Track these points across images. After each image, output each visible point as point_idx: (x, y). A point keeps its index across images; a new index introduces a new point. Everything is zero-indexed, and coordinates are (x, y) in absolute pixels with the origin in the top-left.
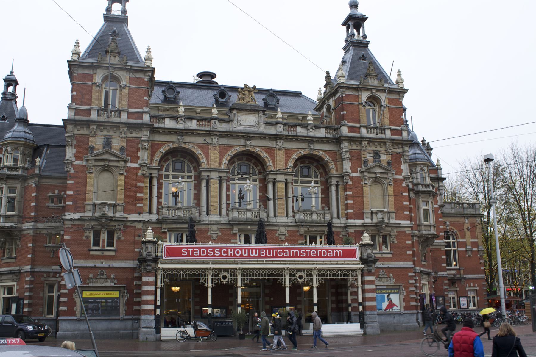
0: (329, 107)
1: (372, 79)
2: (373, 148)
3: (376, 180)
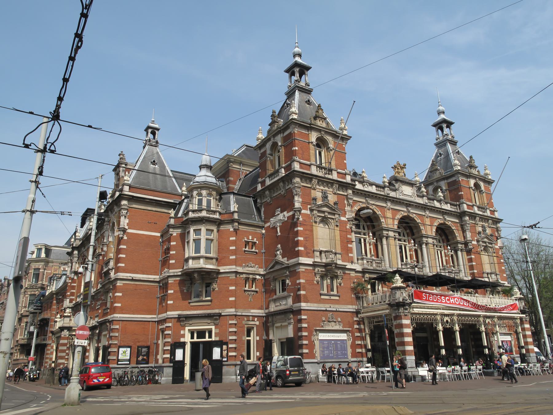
0: (275, 145)
1: (321, 121)
2: (322, 188)
3: (324, 220)
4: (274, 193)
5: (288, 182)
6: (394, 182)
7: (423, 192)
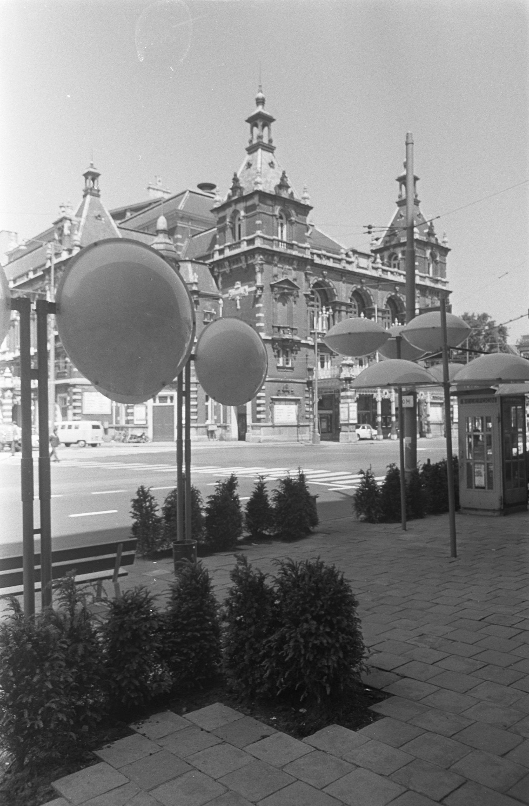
4: (234, 264)
5: (251, 257)
6: (350, 253)
7: (378, 263)
